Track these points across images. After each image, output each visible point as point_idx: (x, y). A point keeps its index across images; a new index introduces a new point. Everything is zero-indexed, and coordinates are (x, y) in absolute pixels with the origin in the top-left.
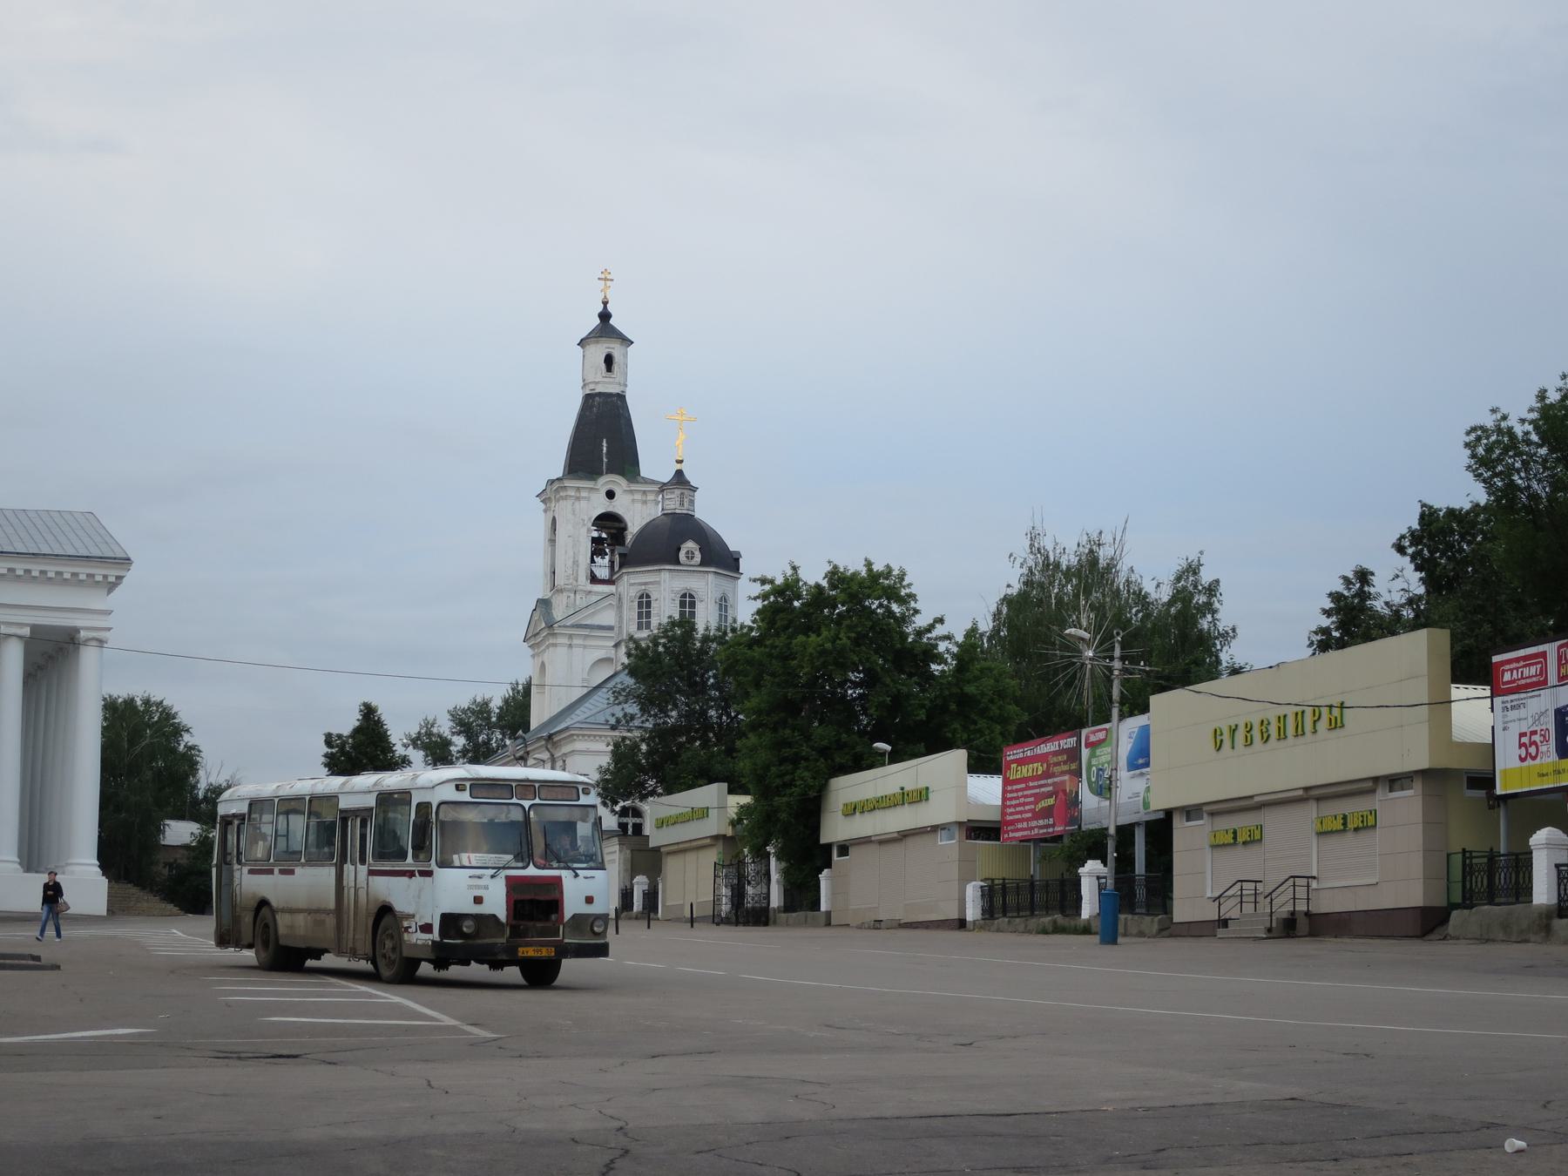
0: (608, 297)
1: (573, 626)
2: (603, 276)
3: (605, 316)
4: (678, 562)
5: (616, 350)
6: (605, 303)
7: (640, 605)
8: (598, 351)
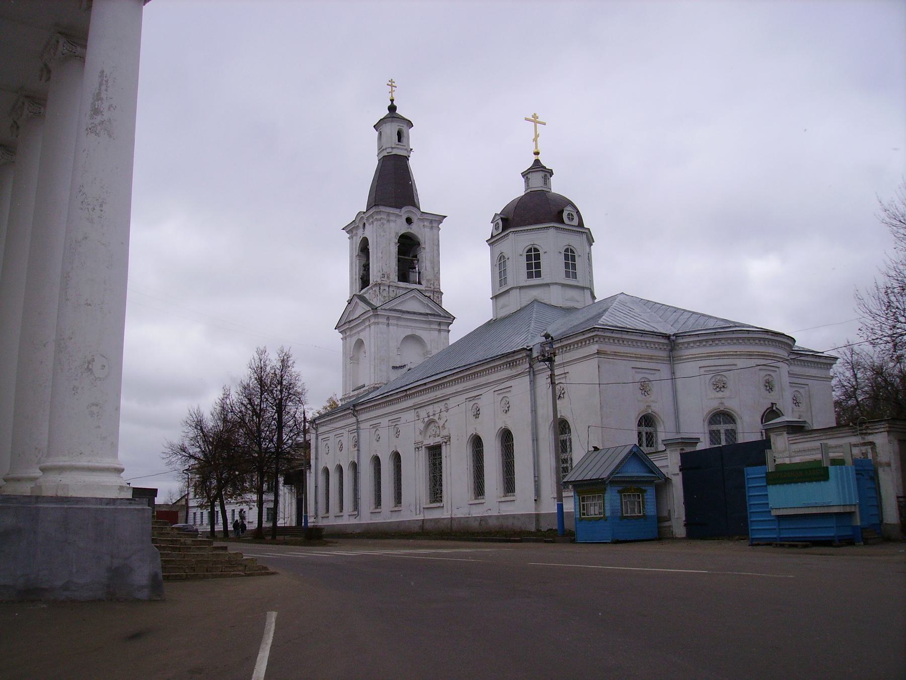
0: (393, 96)
1: (390, 310)
2: (390, 83)
3: (392, 108)
4: (562, 222)
5: (404, 128)
6: (392, 101)
7: (529, 258)
8: (391, 130)
